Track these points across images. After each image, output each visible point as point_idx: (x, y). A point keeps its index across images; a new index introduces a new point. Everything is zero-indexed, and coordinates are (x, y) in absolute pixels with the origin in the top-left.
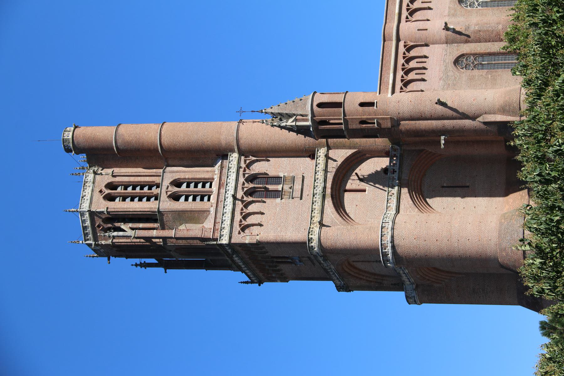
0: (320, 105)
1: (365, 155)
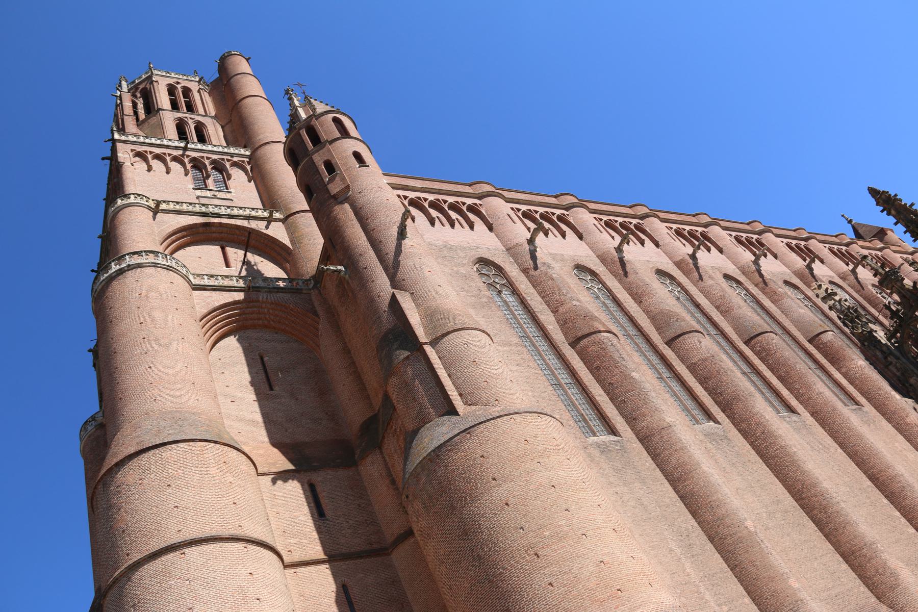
0: (336, 121)
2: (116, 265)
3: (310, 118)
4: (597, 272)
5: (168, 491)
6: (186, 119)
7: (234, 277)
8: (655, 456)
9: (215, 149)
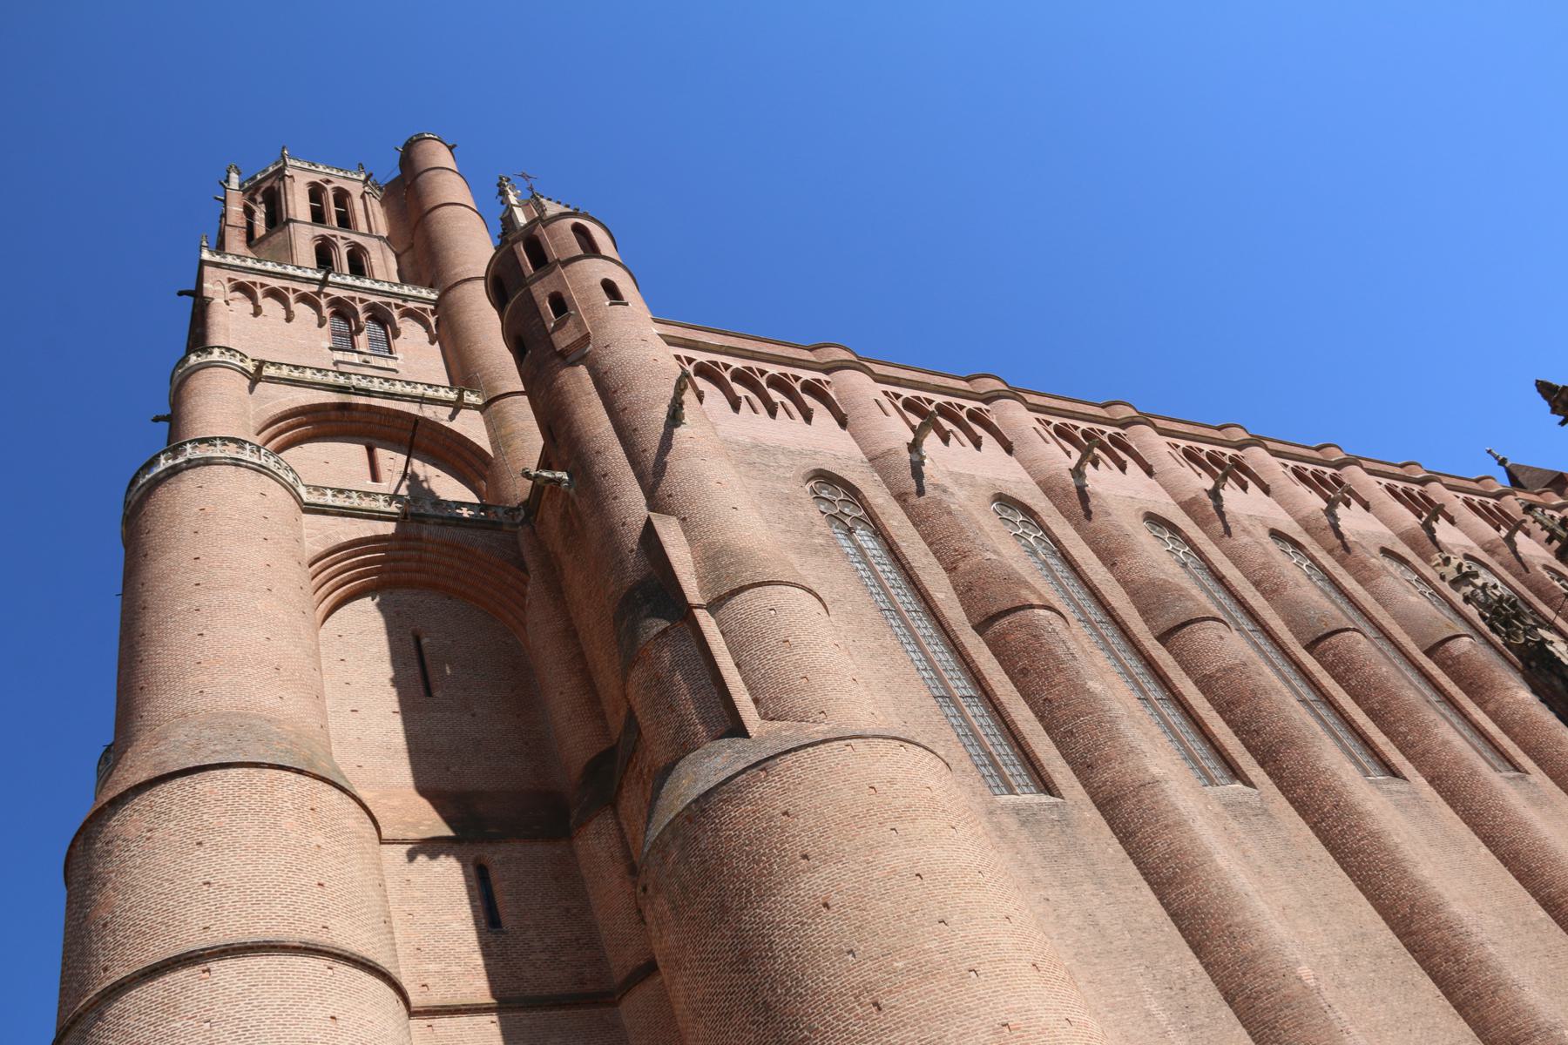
0: (580, 231)
1: (484, 478)
2: (167, 459)
3: (533, 223)
4: (1036, 509)
5: (197, 853)
6: (334, 239)
7: (380, 496)
8: (1126, 835)
9: (377, 286)
